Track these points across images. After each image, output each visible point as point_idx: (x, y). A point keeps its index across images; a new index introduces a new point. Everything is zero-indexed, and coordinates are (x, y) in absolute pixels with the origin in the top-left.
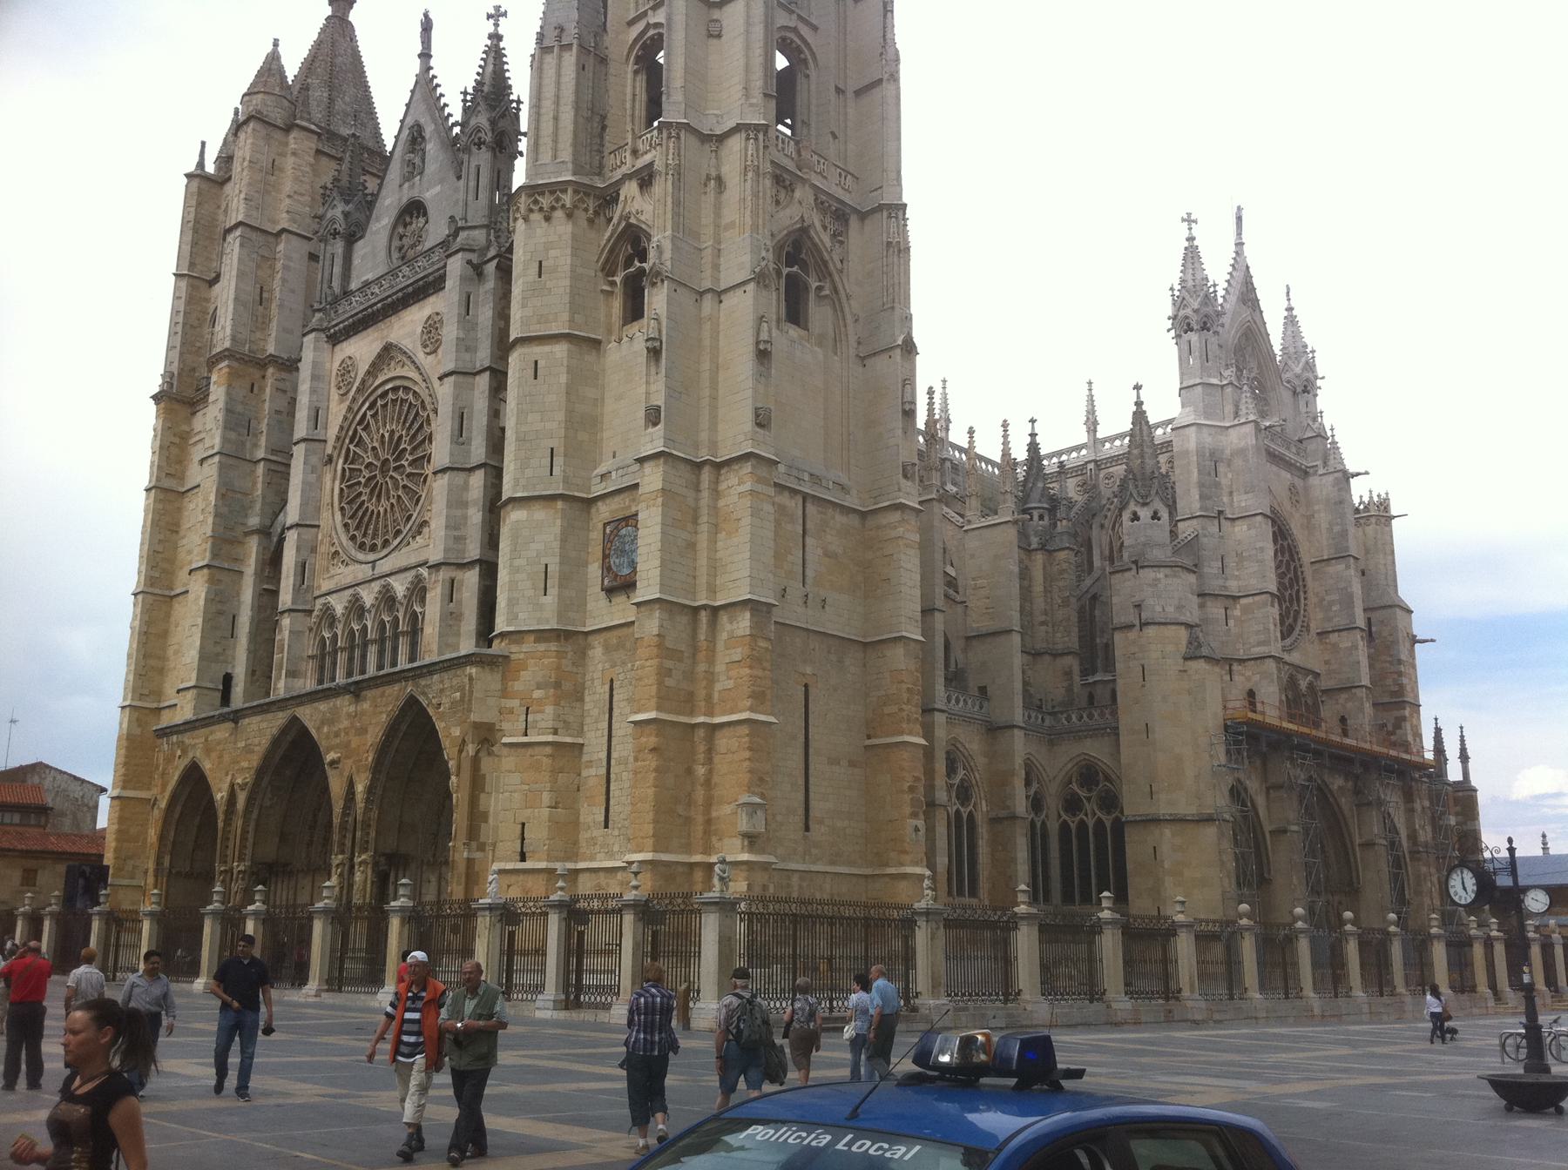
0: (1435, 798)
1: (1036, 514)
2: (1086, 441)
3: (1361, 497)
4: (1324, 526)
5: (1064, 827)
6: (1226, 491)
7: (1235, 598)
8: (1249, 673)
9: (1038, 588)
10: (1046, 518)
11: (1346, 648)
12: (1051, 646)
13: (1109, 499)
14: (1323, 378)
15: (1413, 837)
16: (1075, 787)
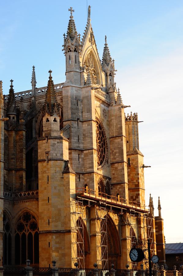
0: (149, 223)
1: (12, 116)
2: (31, 89)
3: (128, 114)
4: (115, 125)
5: (17, 236)
6: (80, 111)
7: (82, 151)
8: (85, 178)
9: (12, 145)
10: (15, 118)
11: (120, 169)
12: (15, 167)
13: (39, 112)
14: (116, 71)
15: (140, 236)
16: (22, 221)
